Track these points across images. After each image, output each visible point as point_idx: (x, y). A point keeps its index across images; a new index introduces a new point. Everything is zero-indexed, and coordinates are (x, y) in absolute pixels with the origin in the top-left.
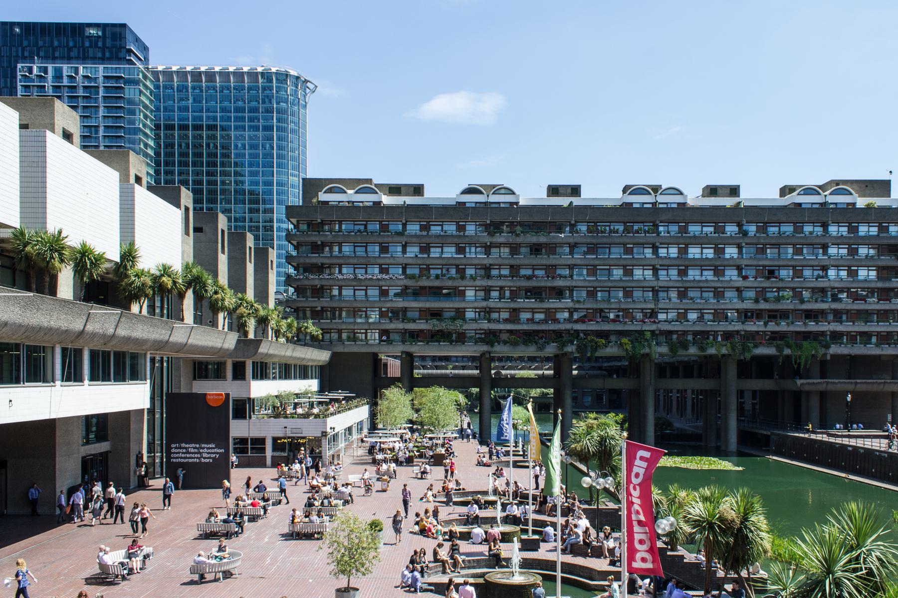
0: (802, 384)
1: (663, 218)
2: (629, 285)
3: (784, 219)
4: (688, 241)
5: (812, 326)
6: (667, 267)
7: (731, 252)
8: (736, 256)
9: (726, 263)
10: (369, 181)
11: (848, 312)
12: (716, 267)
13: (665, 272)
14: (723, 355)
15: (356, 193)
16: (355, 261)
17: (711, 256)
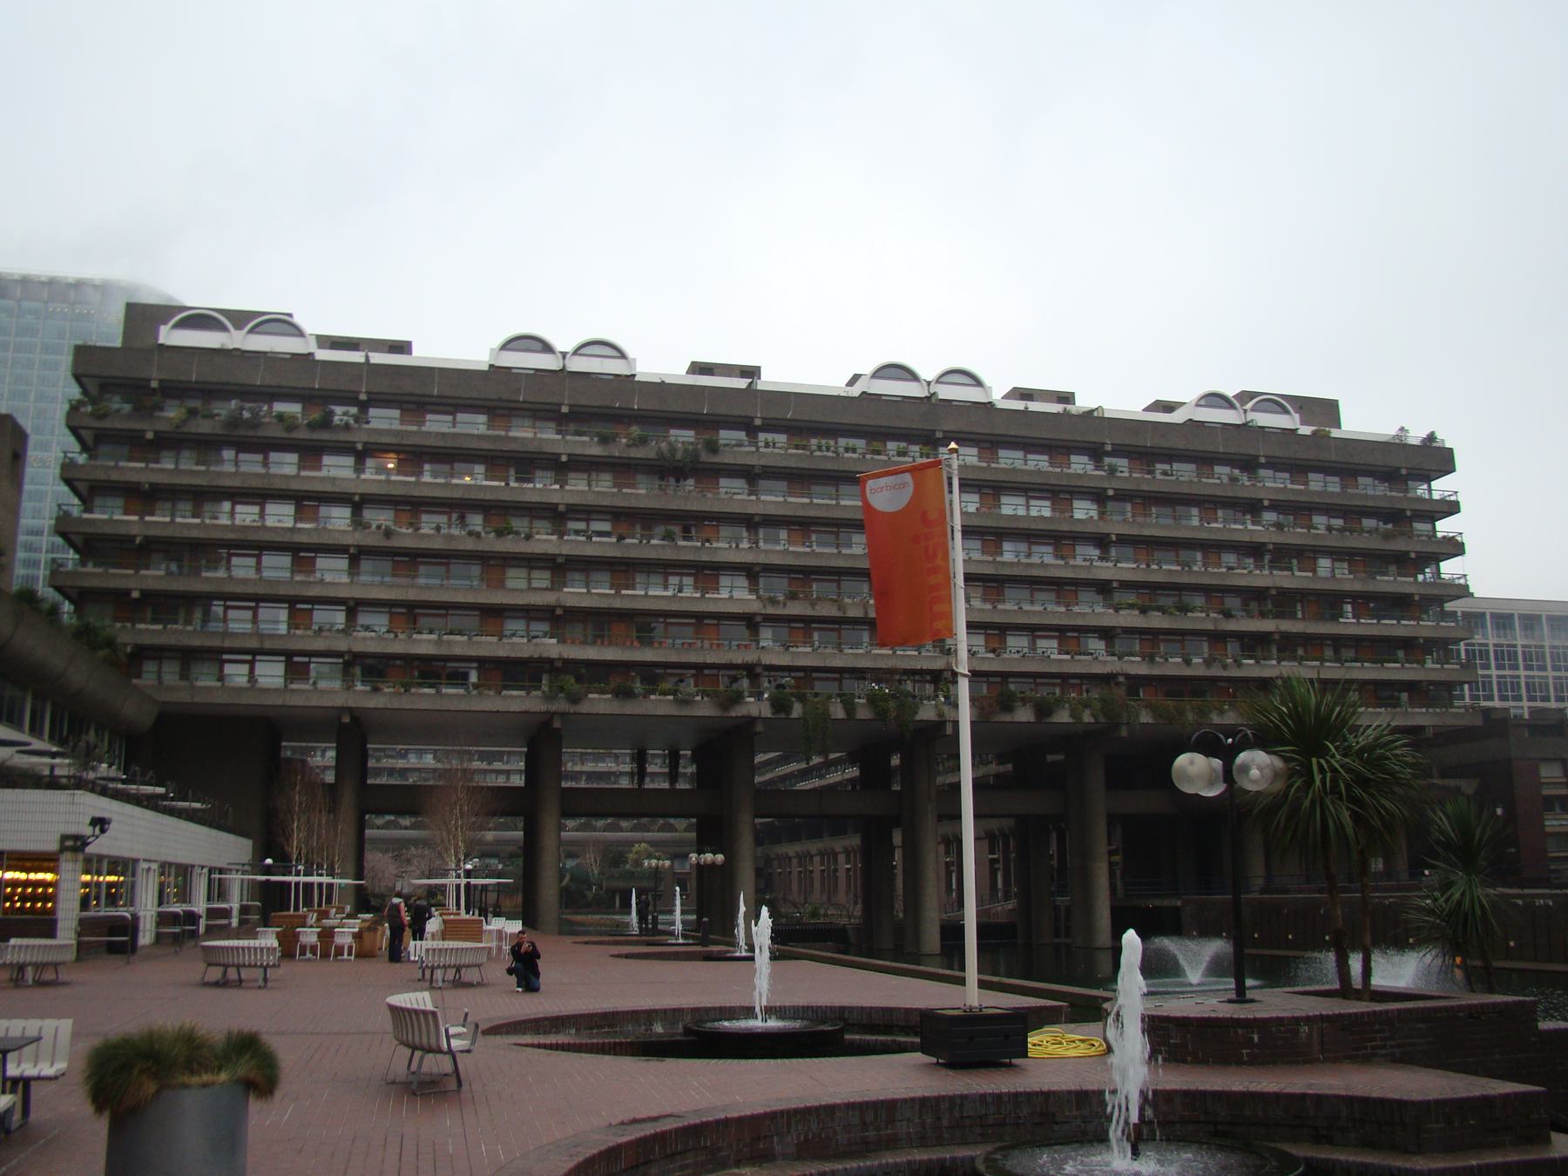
7: (1083, 511)
15: (251, 331)
17: (1047, 513)
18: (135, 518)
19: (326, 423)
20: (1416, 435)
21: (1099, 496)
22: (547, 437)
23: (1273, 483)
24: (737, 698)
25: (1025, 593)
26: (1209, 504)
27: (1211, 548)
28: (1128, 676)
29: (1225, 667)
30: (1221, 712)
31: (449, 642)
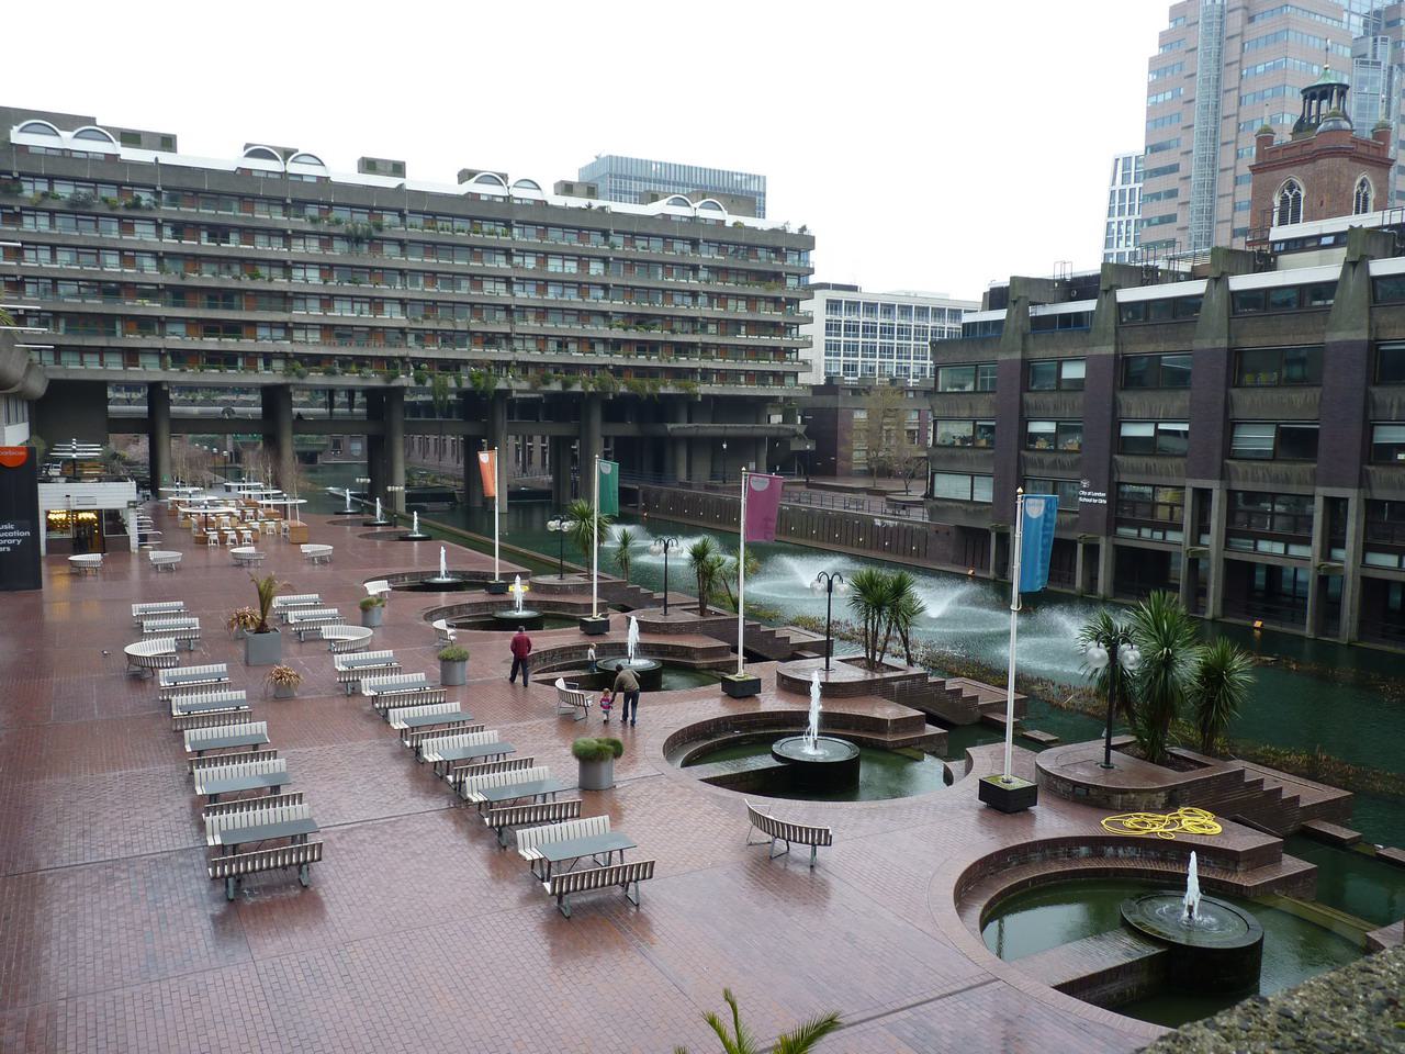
0: (672, 429)
1: (518, 219)
3: (654, 232)
4: (549, 249)
5: (683, 362)
6: (523, 281)
7: (596, 268)
8: (602, 272)
10: (91, 121)
11: (718, 346)
12: (580, 284)
14: (592, 393)
15: (75, 137)
16: (81, 243)
17: (574, 271)
18: (14, 263)
19: (136, 205)
20: (794, 229)
21: (605, 260)
22: (278, 218)
23: (708, 255)
24: (395, 376)
26: (668, 267)
27: (667, 293)
28: (614, 366)
29: (669, 361)
30: (665, 386)
31: (226, 342)
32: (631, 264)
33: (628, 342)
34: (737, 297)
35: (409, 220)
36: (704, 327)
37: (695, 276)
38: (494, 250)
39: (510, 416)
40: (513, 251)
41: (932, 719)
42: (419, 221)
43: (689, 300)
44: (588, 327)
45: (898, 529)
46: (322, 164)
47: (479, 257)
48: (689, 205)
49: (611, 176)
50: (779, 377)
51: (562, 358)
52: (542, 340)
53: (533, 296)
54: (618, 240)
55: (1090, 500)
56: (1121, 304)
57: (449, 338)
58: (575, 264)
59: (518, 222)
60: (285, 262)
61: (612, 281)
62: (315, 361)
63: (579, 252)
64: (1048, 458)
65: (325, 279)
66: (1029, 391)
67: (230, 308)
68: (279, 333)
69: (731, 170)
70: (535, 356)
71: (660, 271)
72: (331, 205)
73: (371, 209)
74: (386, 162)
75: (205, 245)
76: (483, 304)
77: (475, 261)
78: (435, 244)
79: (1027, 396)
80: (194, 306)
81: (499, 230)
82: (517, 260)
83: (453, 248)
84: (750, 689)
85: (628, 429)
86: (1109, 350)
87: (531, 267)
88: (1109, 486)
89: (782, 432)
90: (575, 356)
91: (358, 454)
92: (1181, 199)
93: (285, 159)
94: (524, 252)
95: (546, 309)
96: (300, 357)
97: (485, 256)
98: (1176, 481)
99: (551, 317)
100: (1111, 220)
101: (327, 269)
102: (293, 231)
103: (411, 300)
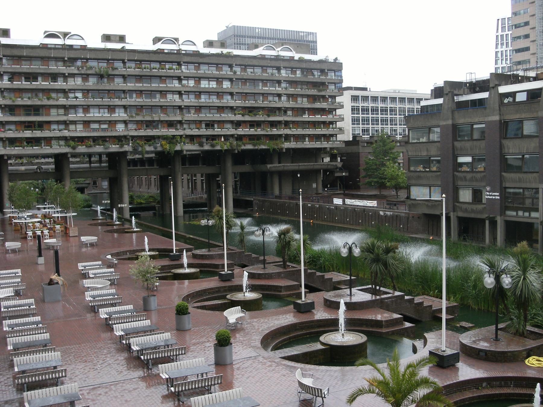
1: (185, 60)
2: (165, 104)
5: (275, 131)
6: (188, 93)
7: (226, 85)
8: (229, 86)
9: (224, 91)
11: (293, 122)
12: (218, 93)
13: (187, 96)
14: (226, 150)
17: (215, 86)
21: (231, 80)
22: (61, 68)
25: (208, 111)
26: (265, 82)
27: (265, 95)
28: (238, 135)
31: (35, 133)
32: (245, 81)
33: (245, 122)
34: (302, 96)
35: (128, 65)
36: (285, 112)
37: (279, 86)
38: (172, 77)
39: (183, 164)
40: (182, 77)
41: (407, 319)
42: (133, 65)
43: (276, 99)
44: (223, 115)
45: (392, 216)
46: (83, 39)
47: (164, 82)
48: (274, 50)
49: (234, 36)
50: (327, 137)
51: (210, 132)
52: (198, 123)
53: (193, 100)
54: (238, 70)
55: (491, 197)
56: (501, 94)
57: (150, 124)
58: (215, 83)
59: (184, 63)
60: (65, 90)
61: (235, 90)
62: (81, 140)
63: (217, 76)
64: (469, 176)
65: (84, 96)
66: (457, 141)
67: (38, 115)
68: (62, 127)
69: (298, 30)
70: (195, 132)
71: (261, 84)
72: (87, 59)
73: (108, 60)
74: (115, 36)
75: (24, 84)
76: (167, 106)
77: (162, 84)
78: (141, 76)
79: (457, 144)
80: (20, 115)
81: (174, 67)
82: (184, 82)
83: (151, 77)
84: (309, 308)
85: (246, 168)
86: (496, 118)
87: (192, 85)
88: (501, 189)
89: (329, 167)
90: (217, 131)
91: (105, 187)
92: (532, 38)
93: (64, 37)
94: (188, 78)
95: (201, 107)
96: (73, 138)
97: (167, 81)
98: (534, 186)
99: (203, 111)
100: (497, 50)
101: (86, 92)
102: (69, 74)
103: (129, 106)
